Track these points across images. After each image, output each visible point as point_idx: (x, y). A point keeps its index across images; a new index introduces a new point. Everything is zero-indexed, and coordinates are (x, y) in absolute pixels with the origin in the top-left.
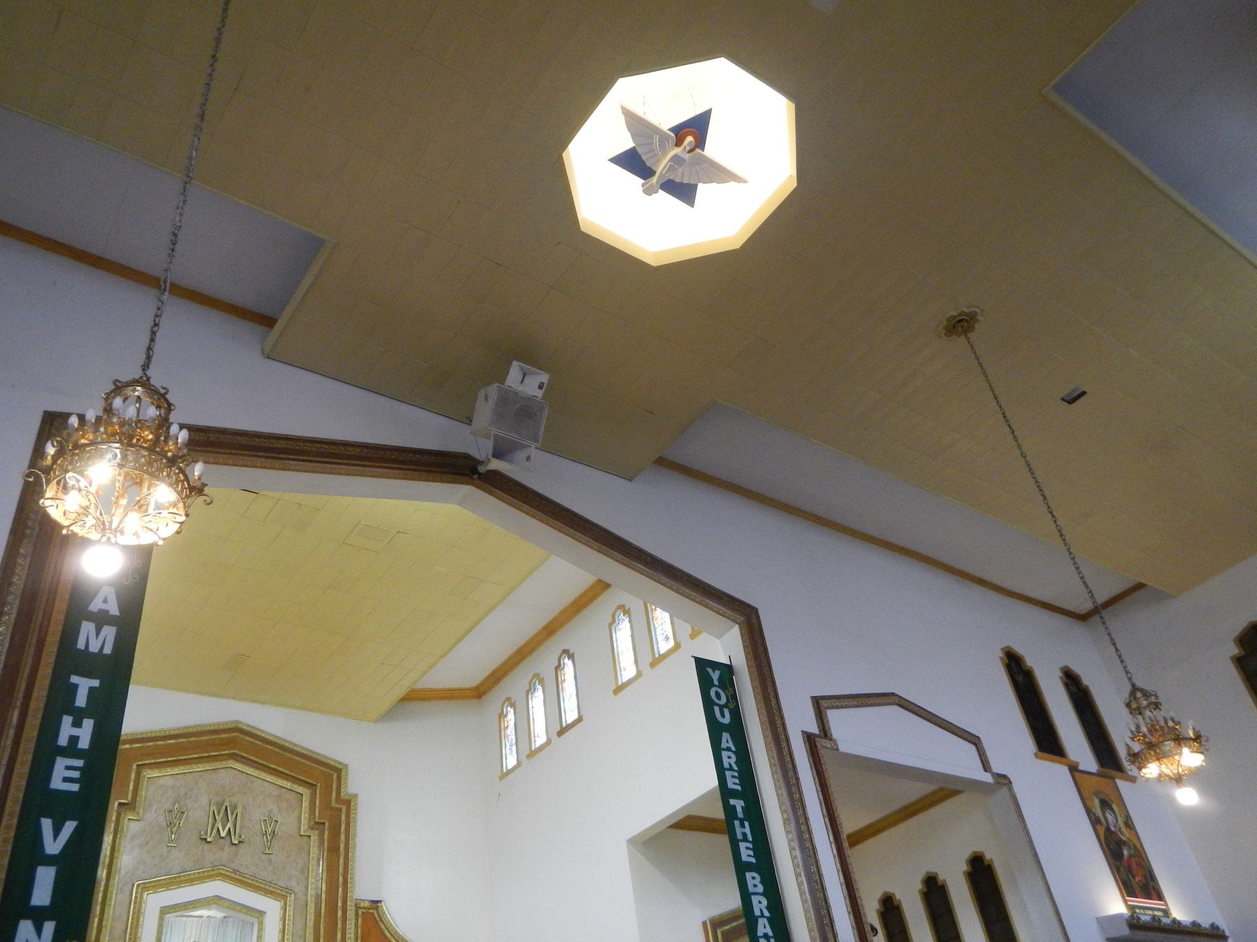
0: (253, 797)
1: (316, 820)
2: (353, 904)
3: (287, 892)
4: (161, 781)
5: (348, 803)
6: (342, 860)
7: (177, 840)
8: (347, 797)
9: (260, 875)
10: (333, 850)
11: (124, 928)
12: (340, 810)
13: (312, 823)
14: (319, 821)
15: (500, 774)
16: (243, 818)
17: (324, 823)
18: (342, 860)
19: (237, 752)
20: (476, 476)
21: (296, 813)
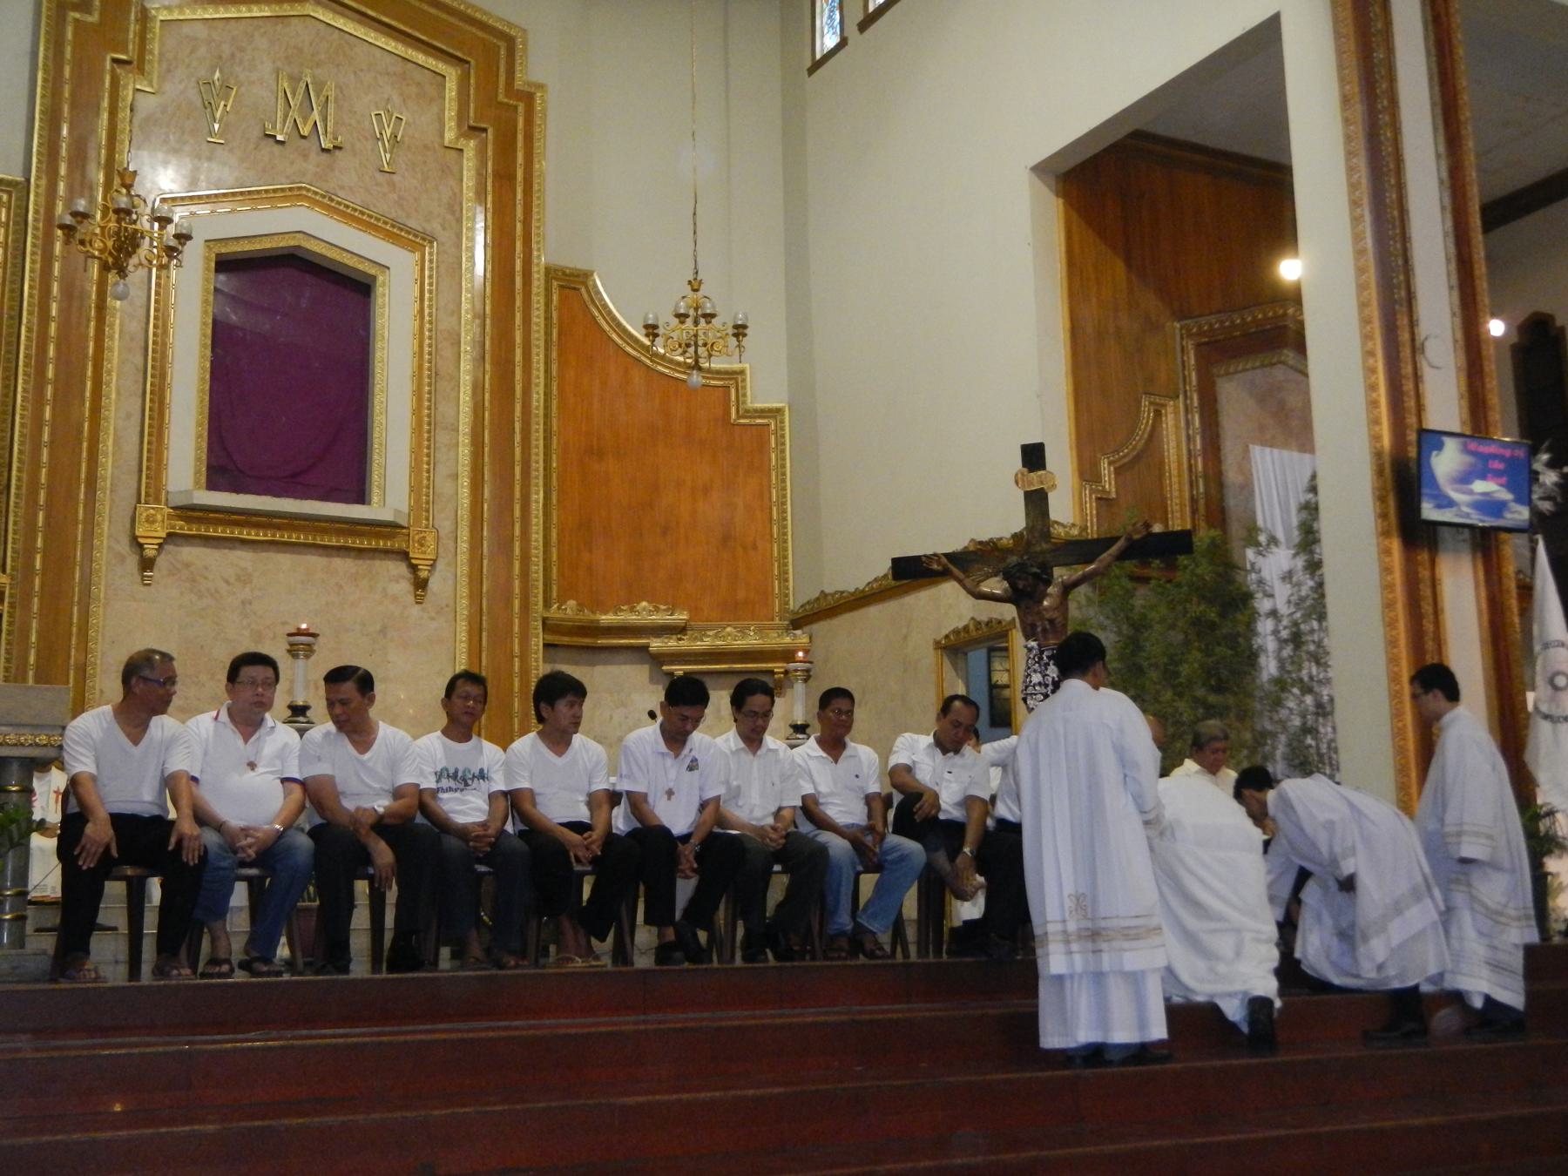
0: (355, 73)
1: (472, 123)
2: (543, 271)
3: (424, 239)
4: (186, 29)
5: (529, 98)
6: (519, 196)
7: (222, 134)
8: (526, 88)
9: (375, 206)
10: (504, 177)
12: (516, 107)
15: (808, 64)
16: (339, 107)
17: (485, 130)
18: (519, 196)
21: (435, 109)
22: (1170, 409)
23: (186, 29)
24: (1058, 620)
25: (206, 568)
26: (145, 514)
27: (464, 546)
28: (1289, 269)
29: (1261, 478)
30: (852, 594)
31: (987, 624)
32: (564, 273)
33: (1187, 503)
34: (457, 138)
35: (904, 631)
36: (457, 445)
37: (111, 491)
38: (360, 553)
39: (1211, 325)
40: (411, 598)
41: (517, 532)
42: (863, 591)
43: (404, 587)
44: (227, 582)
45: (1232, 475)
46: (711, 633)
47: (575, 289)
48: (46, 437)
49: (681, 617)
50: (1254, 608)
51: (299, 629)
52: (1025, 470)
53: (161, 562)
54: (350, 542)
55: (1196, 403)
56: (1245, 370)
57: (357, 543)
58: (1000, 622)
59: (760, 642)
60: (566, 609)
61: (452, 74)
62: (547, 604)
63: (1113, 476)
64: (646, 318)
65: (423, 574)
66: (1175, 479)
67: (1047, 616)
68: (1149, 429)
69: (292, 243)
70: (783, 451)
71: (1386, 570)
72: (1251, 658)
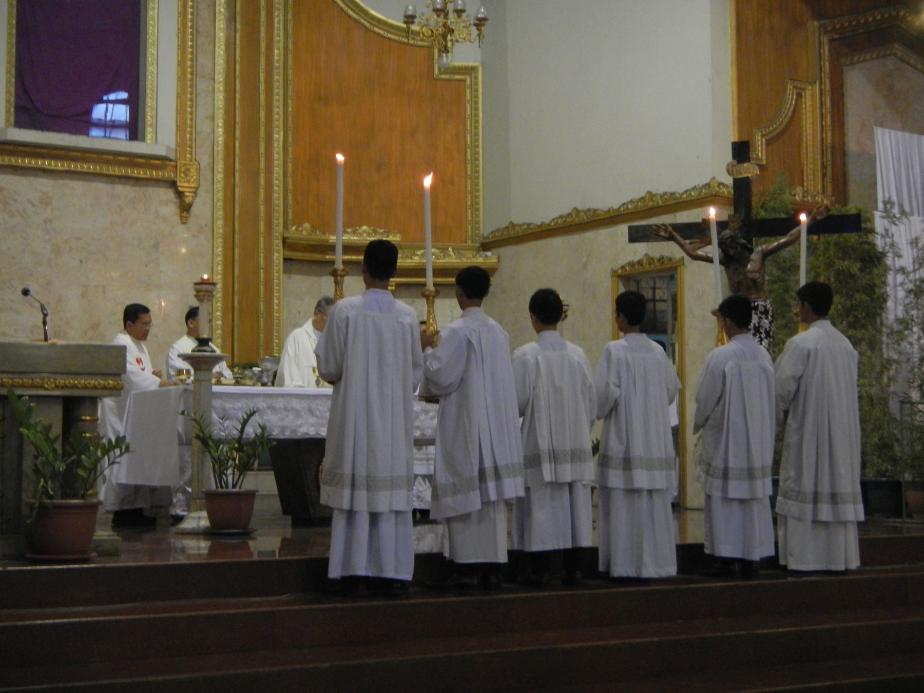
22: (808, 92)
24: (759, 280)
25: (15, 192)
27: (219, 177)
29: (882, 152)
30: (539, 227)
31: (659, 260)
33: (819, 169)
35: (585, 259)
38: (137, 181)
39: (842, 25)
40: (177, 219)
41: (262, 165)
42: (549, 225)
43: (171, 210)
44: (33, 205)
45: (852, 146)
46: (419, 253)
50: (886, 265)
51: (202, 279)
54: (129, 172)
55: (828, 87)
56: (864, 60)
57: (136, 173)
58: (670, 259)
59: (459, 261)
60: (302, 231)
62: (286, 227)
63: (764, 146)
64: (407, 9)
65: (188, 200)
66: (810, 149)
67: (750, 276)
68: (792, 108)
70: (477, 103)
72: (878, 302)
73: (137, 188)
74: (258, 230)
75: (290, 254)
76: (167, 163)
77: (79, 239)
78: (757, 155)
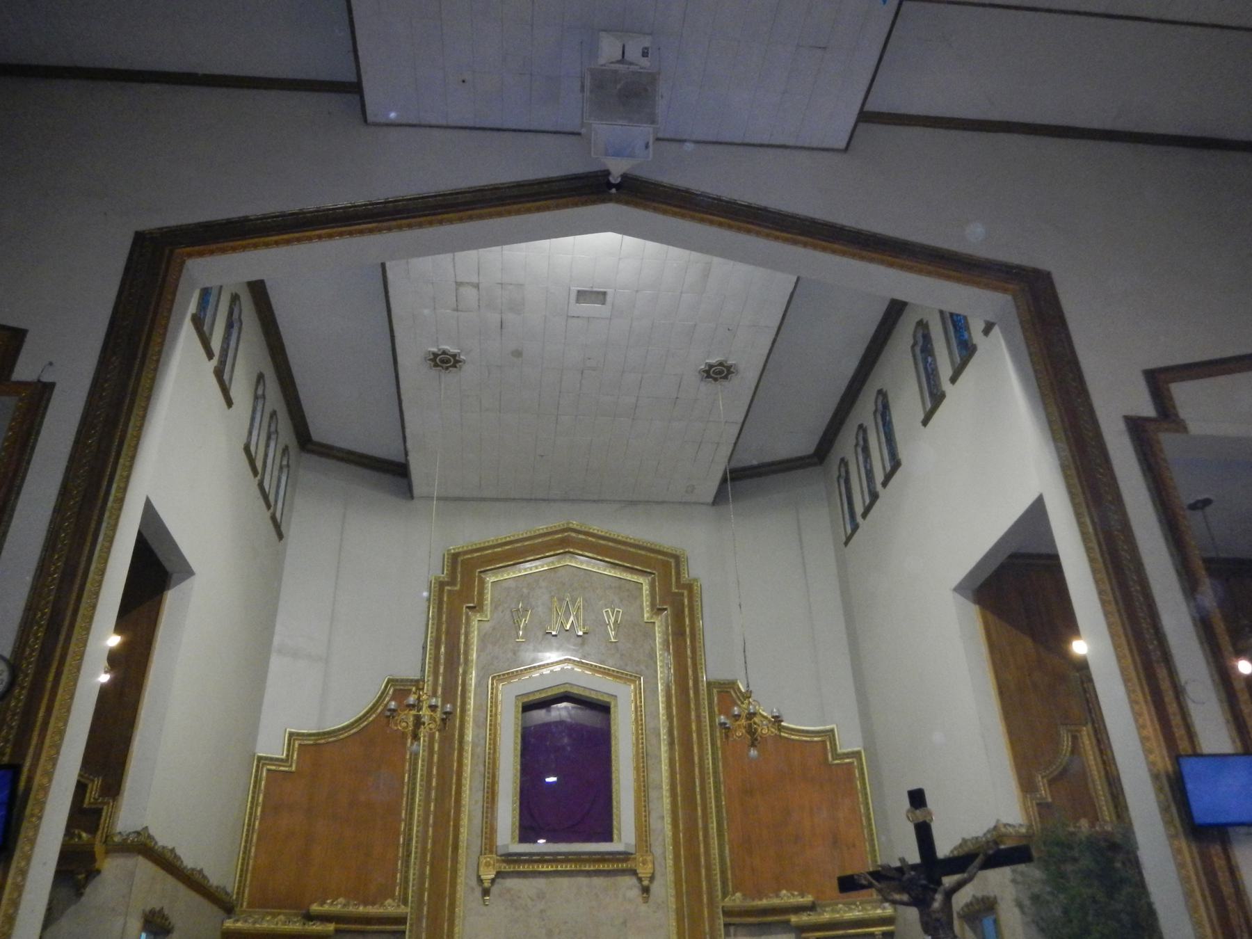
5: (690, 587)
11: (485, 716)
13: (655, 610)
14: (660, 607)
15: (844, 539)
19: (572, 550)
20: (614, 191)
23: (505, 585)
26: (484, 861)
27: (670, 862)
28: (1079, 647)
32: (720, 683)
34: (652, 617)
36: (662, 797)
37: (467, 848)
40: (640, 900)
43: (635, 893)
44: (532, 900)
47: (727, 692)
48: (431, 821)
49: (808, 899)
52: (913, 809)
53: (495, 890)
61: (644, 582)
62: (725, 895)
67: (937, 915)
68: (1069, 749)
69: (562, 690)
71: (1181, 866)
73: (609, 879)
74: (701, 901)
75: (729, 920)
76: (630, 856)
77: (566, 923)
78: (1041, 794)
